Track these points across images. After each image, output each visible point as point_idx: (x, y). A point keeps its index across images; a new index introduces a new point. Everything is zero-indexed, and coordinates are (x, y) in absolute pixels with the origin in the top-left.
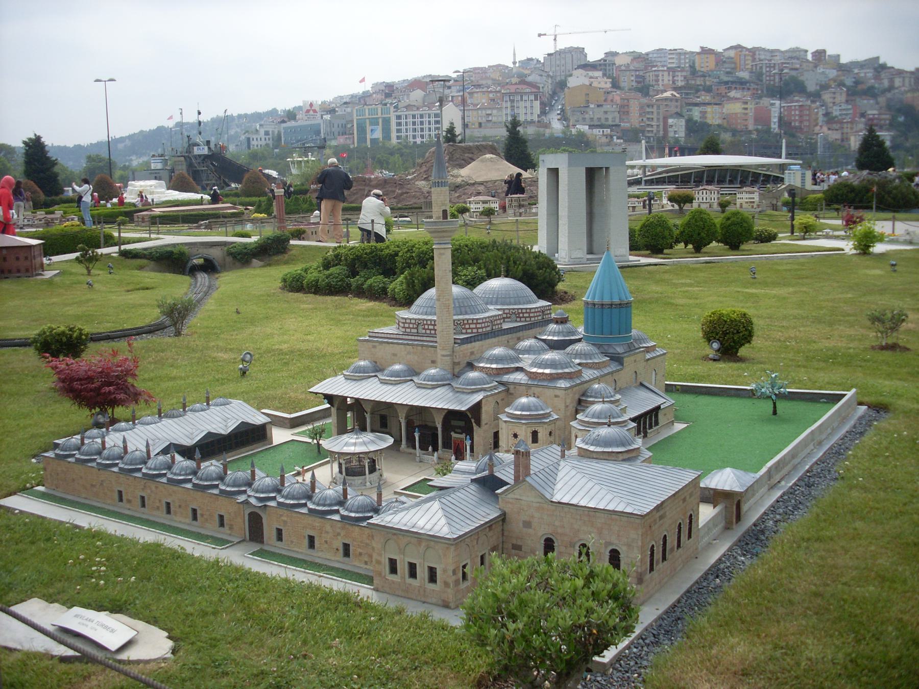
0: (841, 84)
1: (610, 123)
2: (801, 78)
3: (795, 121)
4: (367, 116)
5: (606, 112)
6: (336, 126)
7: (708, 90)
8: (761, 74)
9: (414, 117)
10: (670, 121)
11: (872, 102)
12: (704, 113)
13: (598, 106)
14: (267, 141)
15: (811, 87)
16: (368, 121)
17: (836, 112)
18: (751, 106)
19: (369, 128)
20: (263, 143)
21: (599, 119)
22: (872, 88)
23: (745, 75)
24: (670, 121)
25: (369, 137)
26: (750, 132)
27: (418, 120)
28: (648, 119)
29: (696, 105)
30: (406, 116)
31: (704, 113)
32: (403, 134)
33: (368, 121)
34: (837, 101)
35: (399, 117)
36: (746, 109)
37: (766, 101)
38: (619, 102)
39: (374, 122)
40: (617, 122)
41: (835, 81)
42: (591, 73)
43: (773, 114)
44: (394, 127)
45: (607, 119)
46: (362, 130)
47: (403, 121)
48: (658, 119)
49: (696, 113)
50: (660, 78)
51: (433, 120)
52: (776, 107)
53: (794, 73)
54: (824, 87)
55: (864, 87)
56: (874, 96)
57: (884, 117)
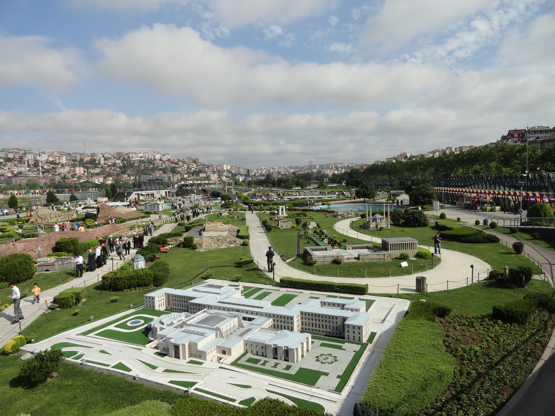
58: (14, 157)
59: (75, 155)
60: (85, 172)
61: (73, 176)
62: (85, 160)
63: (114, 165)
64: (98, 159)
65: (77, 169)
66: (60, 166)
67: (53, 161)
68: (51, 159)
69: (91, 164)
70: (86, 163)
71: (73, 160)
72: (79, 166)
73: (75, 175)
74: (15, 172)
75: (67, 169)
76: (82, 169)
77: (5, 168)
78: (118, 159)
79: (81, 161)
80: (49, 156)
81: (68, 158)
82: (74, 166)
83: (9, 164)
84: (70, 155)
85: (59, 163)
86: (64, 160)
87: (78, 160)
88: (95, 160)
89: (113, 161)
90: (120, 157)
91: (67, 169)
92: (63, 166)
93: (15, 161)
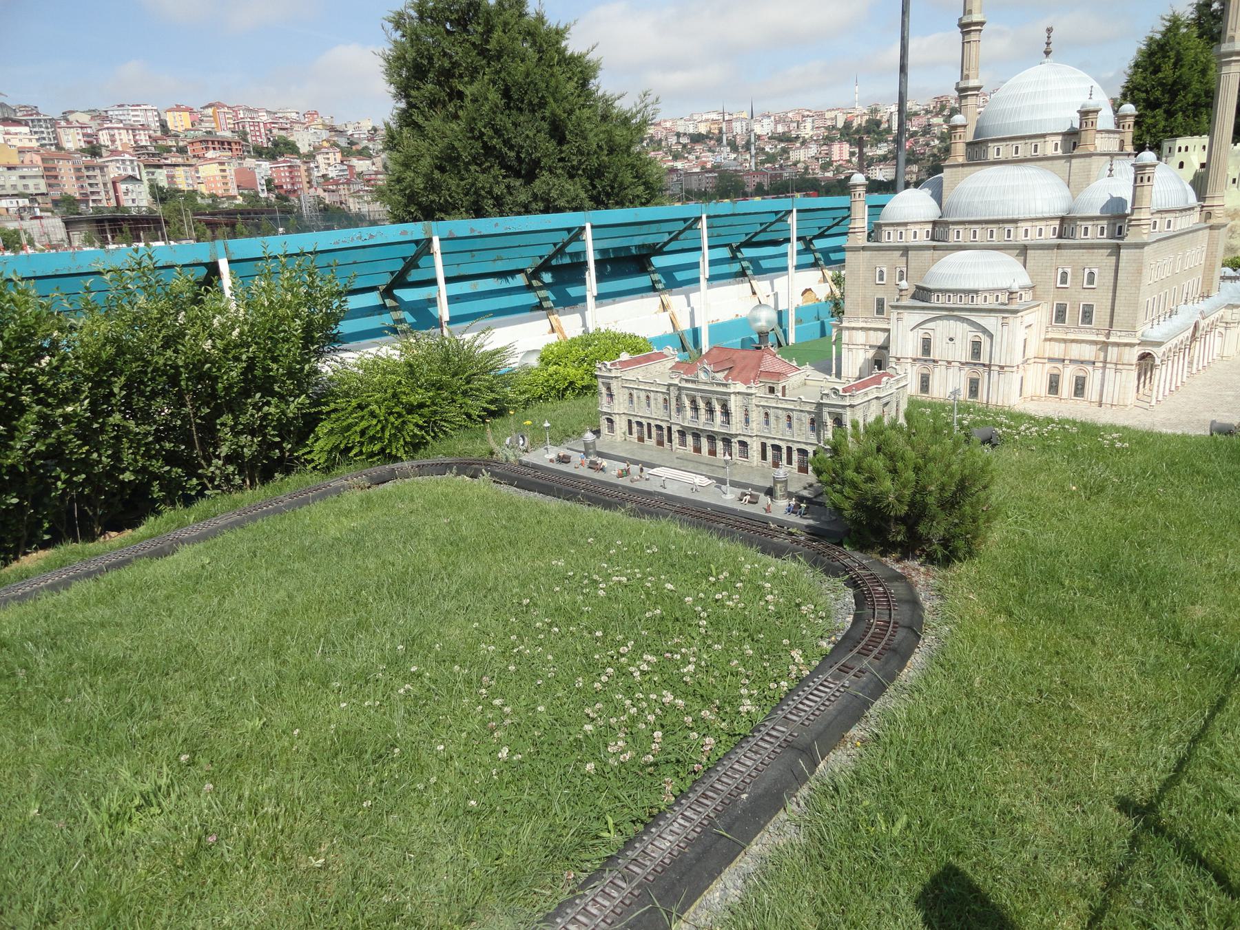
0: (338, 146)
1: (32, 190)
2: (291, 139)
3: (286, 183)
5: (23, 177)
7: (182, 151)
8: (245, 134)
10: (122, 187)
11: (368, 162)
12: (171, 178)
13: (9, 168)
15: (304, 149)
17: (332, 173)
18: (231, 169)
21: (14, 186)
22: (366, 148)
23: (228, 134)
24: (122, 187)
26: (234, 197)
28: (91, 185)
29: (159, 167)
31: (171, 178)
34: (332, 161)
36: (224, 171)
37: (250, 162)
38: (40, 163)
40: (43, 189)
41: (328, 141)
42: (13, 129)
43: (258, 177)
45: (26, 186)
48: (105, 185)
49: (161, 177)
50: (117, 137)
52: (264, 168)
53: (283, 133)
54: (317, 149)
55: (359, 147)
56: (370, 157)
57: (380, 177)
58: (709, 132)
59: (832, 115)
60: (852, 154)
61: (825, 167)
62: (855, 124)
63: (927, 130)
64: (885, 119)
65: (836, 148)
66: (798, 145)
67: (784, 133)
68: (780, 129)
69: (868, 132)
70: (857, 131)
71: (827, 128)
72: (841, 141)
73: (830, 163)
74: (709, 166)
75: (813, 150)
76: (846, 147)
77: (691, 157)
78: (937, 115)
79: (848, 125)
80: (777, 122)
81: (819, 123)
82: (828, 140)
83: (698, 147)
84: (821, 115)
85: (797, 138)
86: (807, 131)
87: (840, 124)
88: (878, 123)
89: (923, 121)
90: (943, 108)
91: (813, 150)
92: (804, 143)
93: (711, 139)
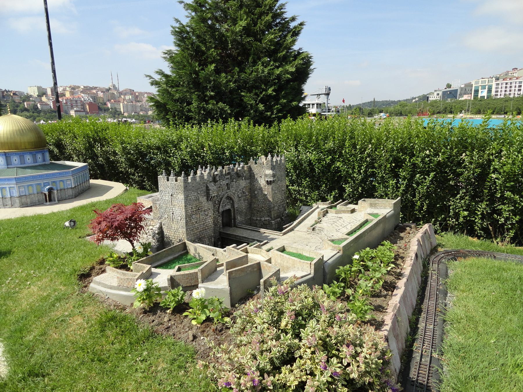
4: (480, 84)
6: (467, 90)
9: (507, 84)
14: (438, 98)
16: (480, 87)
19: (480, 91)
20: (435, 99)
25: (480, 95)
27: (508, 86)
30: (502, 83)
32: (507, 93)
33: (480, 87)
35: (498, 84)
39: (483, 87)
44: (494, 90)
46: (477, 91)
47: (500, 86)
51: (517, 85)
